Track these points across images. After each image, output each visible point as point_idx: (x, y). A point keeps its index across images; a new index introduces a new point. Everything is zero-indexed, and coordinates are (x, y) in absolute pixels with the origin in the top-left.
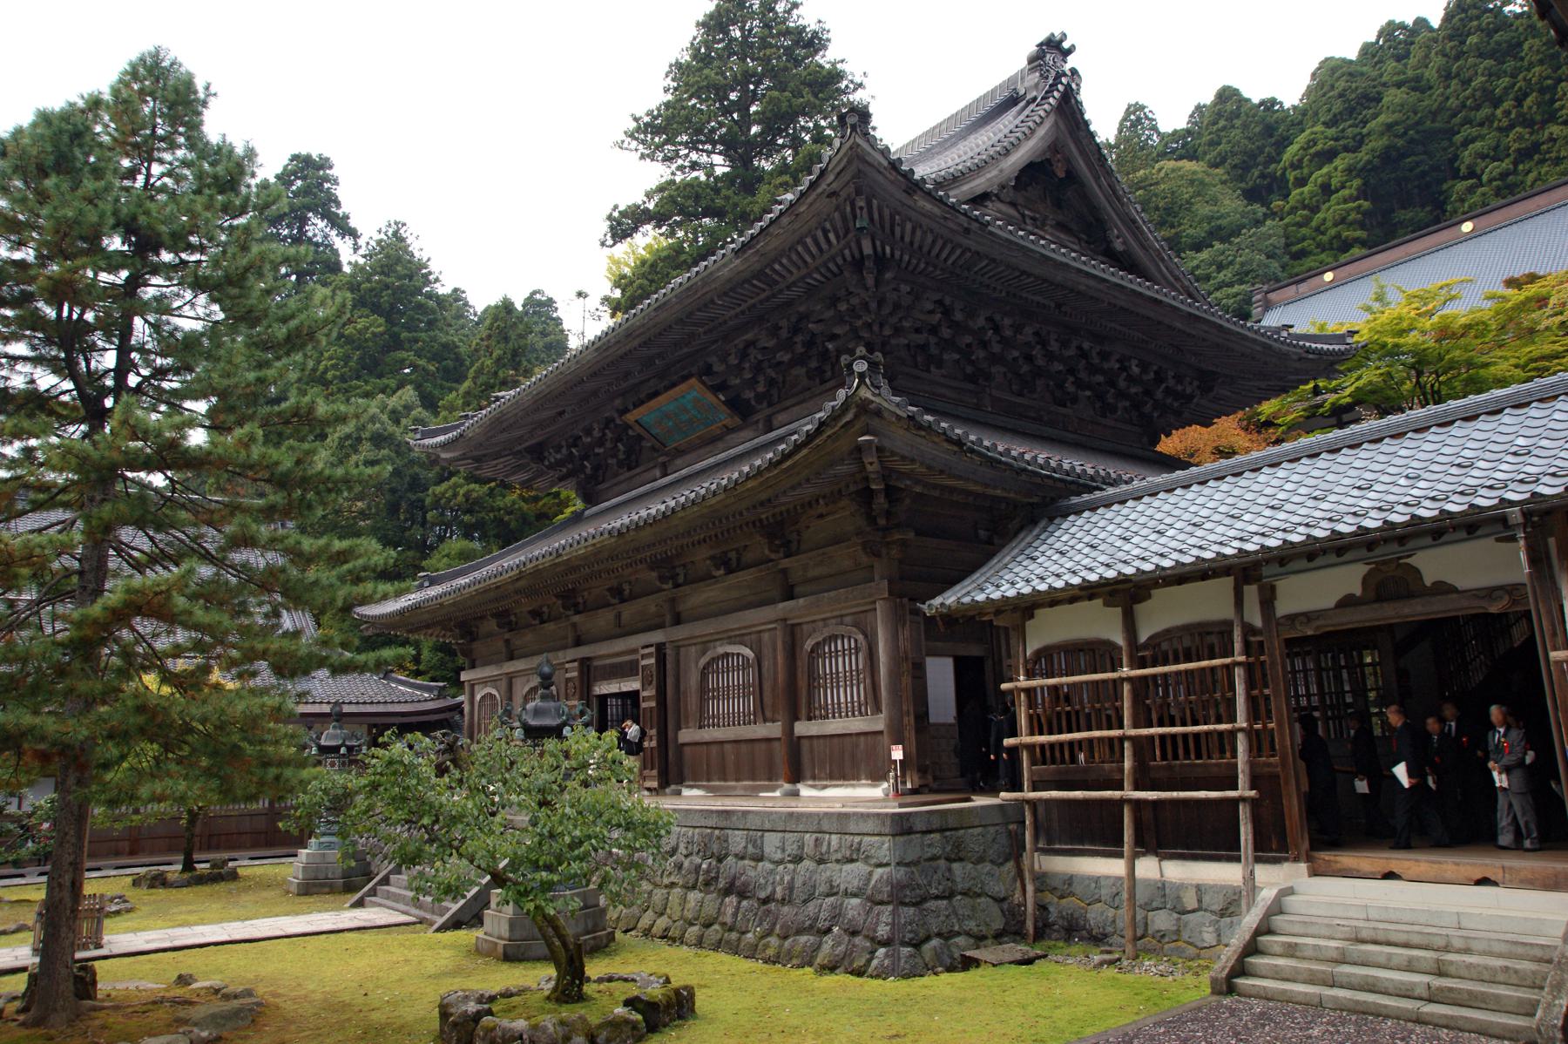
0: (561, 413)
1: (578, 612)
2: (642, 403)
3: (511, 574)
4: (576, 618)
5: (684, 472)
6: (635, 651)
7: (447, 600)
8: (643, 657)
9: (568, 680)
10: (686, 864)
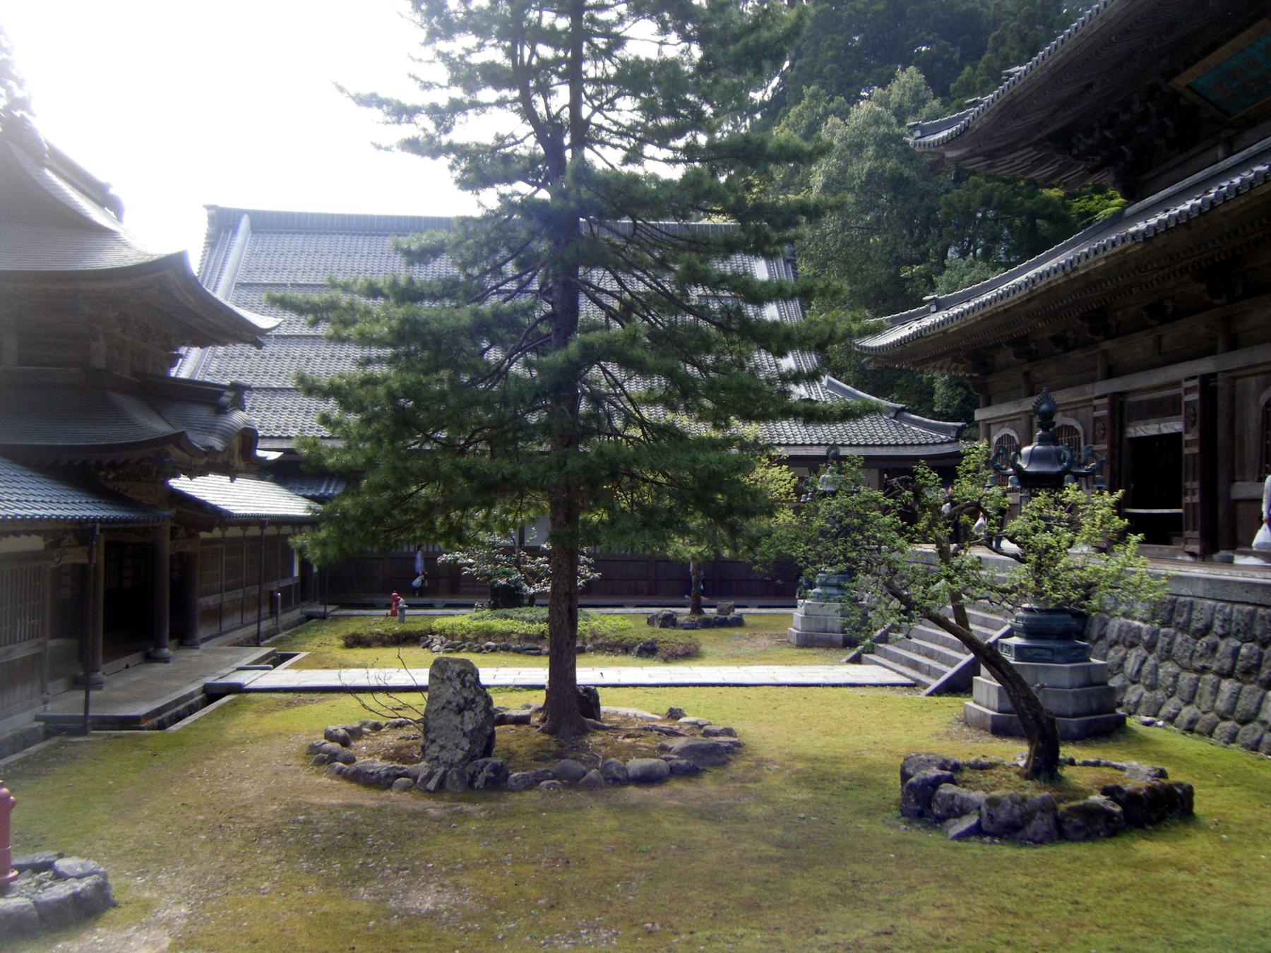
0: (1089, 86)
1: (1108, 337)
2: (1196, 60)
3: (1019, 294)
4: (1107, 345)
5: (1254, 148)
6: (1177, 384)
7: (952, 327)
8: (1188, 391)
9: (1096, 420)
10: (1222, 646)
